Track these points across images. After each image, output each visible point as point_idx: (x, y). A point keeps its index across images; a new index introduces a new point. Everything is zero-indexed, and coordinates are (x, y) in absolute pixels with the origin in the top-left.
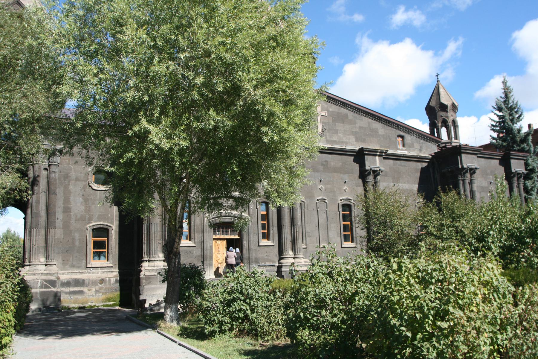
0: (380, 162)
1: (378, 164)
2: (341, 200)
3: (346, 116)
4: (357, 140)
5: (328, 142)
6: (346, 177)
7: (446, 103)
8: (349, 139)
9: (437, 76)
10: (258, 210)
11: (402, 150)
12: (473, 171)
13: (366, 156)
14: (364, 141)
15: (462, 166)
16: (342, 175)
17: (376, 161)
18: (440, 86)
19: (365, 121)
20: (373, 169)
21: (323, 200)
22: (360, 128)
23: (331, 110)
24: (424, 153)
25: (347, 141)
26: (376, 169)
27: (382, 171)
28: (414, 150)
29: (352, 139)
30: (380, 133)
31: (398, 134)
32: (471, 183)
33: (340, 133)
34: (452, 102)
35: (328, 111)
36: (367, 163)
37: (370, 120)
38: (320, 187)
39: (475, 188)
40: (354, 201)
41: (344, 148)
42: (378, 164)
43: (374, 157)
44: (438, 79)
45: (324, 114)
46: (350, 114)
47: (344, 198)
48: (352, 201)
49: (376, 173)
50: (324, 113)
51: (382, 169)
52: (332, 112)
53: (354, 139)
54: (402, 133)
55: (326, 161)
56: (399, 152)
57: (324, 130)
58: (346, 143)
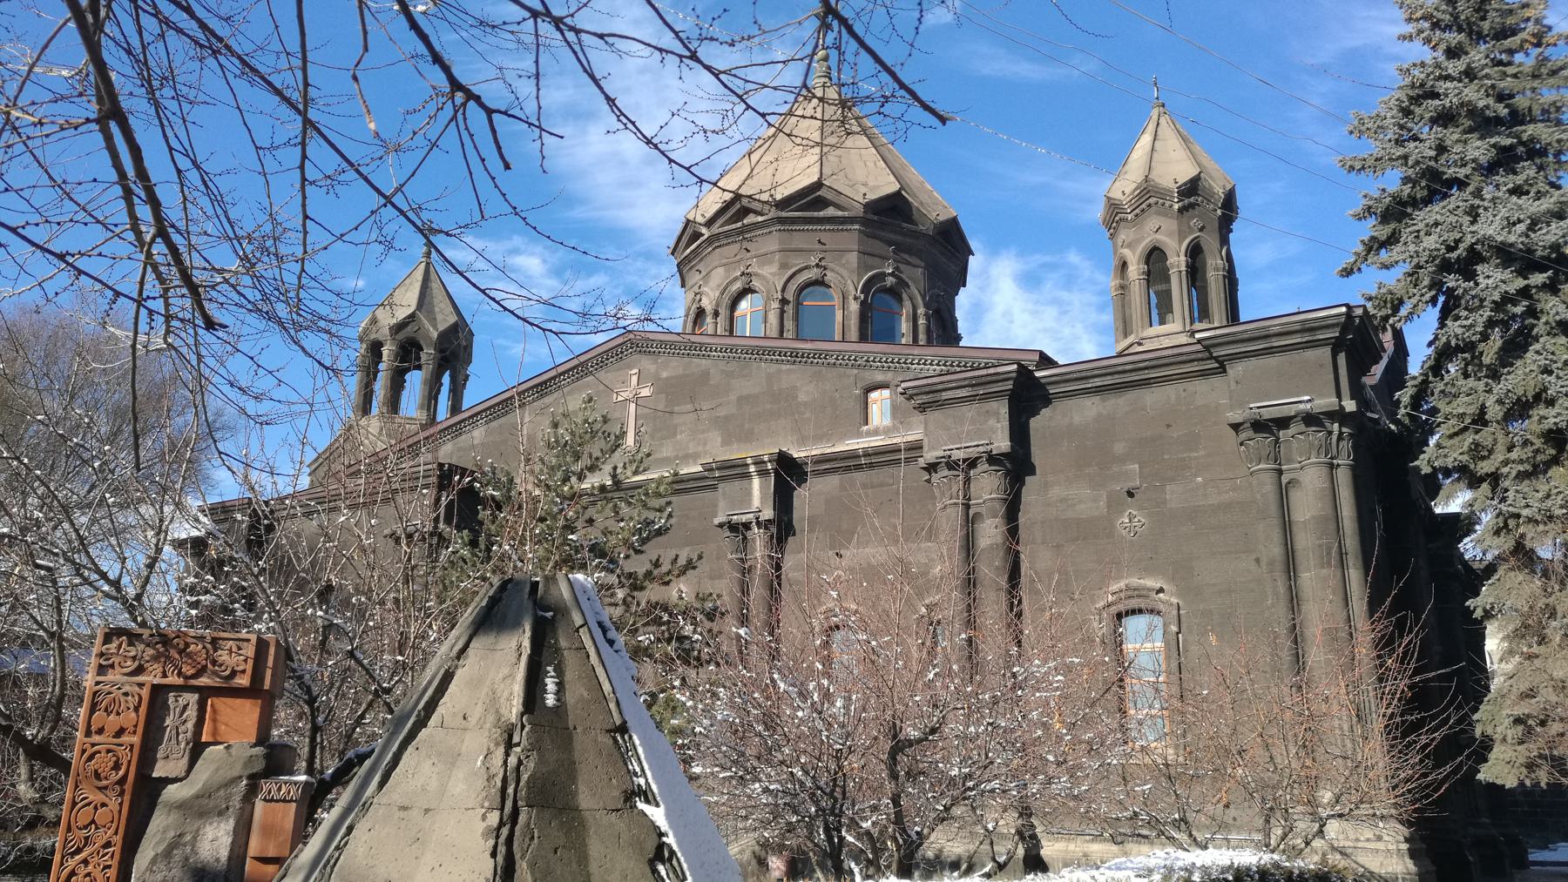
1: (756, 502)
3: (706, 375)
4: (726, 442)
8: (705, 444)
14: (747, 437)
17: (749, 493)
22: (740, 399)
23: (665, 375)
25: (700, 448)
29: (716, 438)
30: (802, 397)
33: (682, 432)
35: (656, 382)
37: (774, 368)
42: (756, 502)
52: (667, 378)
53: (719, 439)
57: (636, 434)
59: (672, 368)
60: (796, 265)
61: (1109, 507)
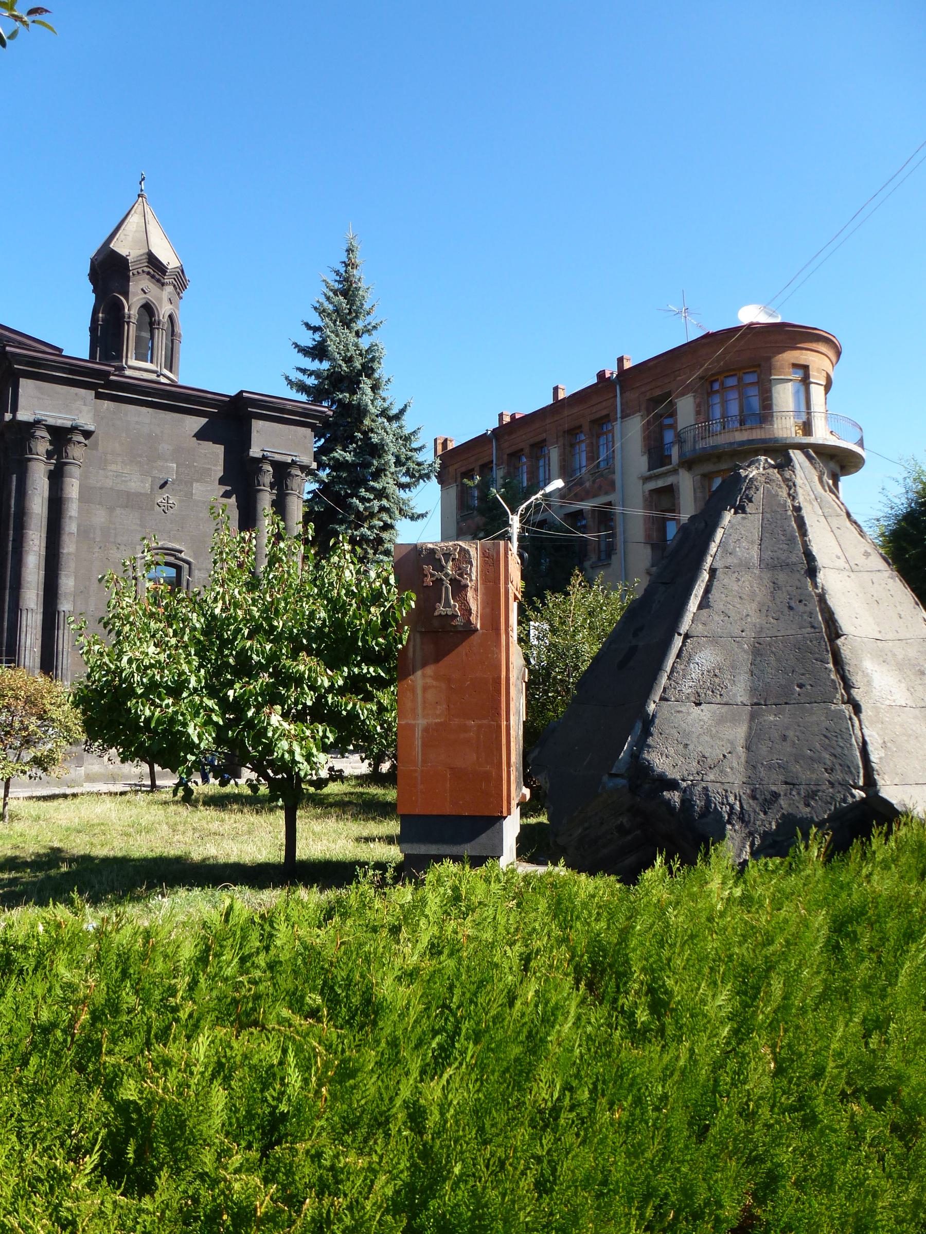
7: (123, 252)
15: (14, 416)
18: (138, 208)
32: (56, 478)
61: (152, 489)
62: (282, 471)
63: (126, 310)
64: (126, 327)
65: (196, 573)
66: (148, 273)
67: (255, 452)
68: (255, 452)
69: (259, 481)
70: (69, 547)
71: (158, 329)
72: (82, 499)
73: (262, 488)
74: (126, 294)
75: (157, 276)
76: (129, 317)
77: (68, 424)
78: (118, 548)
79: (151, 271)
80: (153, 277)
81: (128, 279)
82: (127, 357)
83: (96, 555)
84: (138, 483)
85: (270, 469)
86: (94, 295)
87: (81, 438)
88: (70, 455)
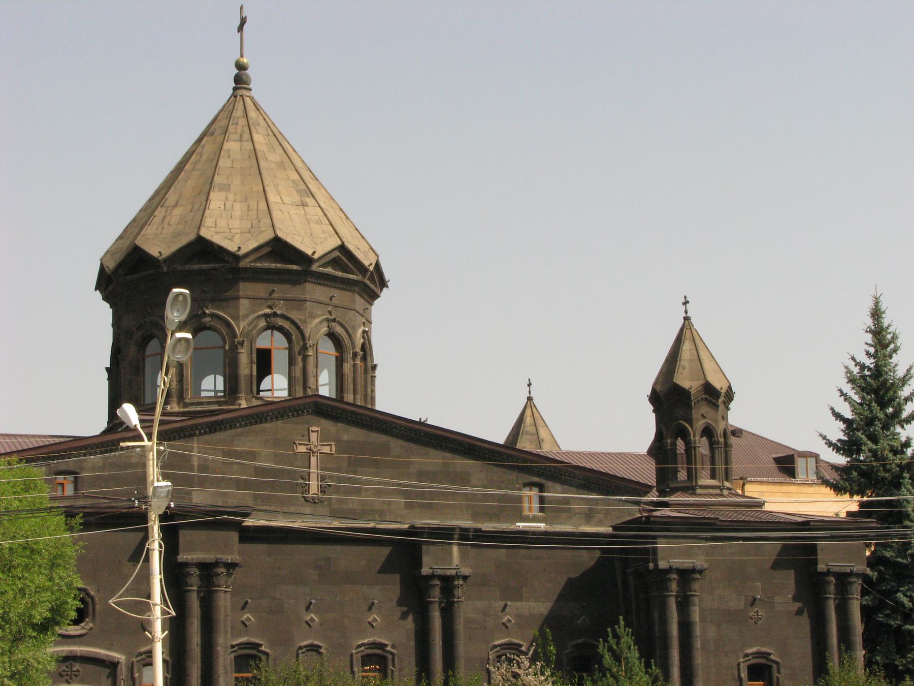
0: (463, 556)
2: (360, 646)
5: (334, 515)
6: (376, 593)
9: (686, 303)
10: (137, 681)
11: (534, 519)
12: (686, 575)
13: (424, 547)
15: (656, 565)
16: (365, 588)
17: (450, 554)
18: (688, 333)
19: (435, 459)
20: (440, 572)
21: (314, 648)
23: (346, 438)
24: (600, 523)
26: (448, 573)
27: (465, 578)
28: (571, 518)
31: (527, 481)
32: (684, 605)
34: (702, 382)
35: (339, 442)
36: (426, 559)
38: (308, 618)
39: (696, 616)
40: (393, 646)
41: (372, 525)
43: (447, 547)
44: (686, 312)
45: (326, 450)
46: (396, 445)
47: (366, 641)
48: (389, 648)
49: (448, 583)
50: (329, 447)
51: (466, 571)
52: (349, 442)
54: (536, 479)
55: (328, 559)
56: (521, 525)
58: (381, 515)
59: (352, 434)
60: (319, 316)
61: (745, 605)
62: (843, 579)
63: (692, 437)
64: (693, 451)
65: (782, 670)
66: (706, 399)
67: (821, 567)
68: (821, 567)
69: (825, 591)
70: (699, 659)
71: (718, 448)
72: (702, 620)
73: (828, 596)
74: (690, 421)
75: (713, 401)
76: (695, 443)
77: (690, 566)
78: (726, 656)
79: (708, 397)
80: (709, 402)
81: (690, 408)
82: (696, 478)
83: (712, 662)
84: (736, 602)
85: (833, 579)
86: (654, 415)
87: (698, 576)
88: (692, 588)
